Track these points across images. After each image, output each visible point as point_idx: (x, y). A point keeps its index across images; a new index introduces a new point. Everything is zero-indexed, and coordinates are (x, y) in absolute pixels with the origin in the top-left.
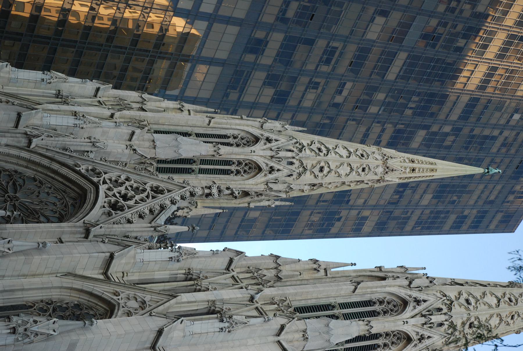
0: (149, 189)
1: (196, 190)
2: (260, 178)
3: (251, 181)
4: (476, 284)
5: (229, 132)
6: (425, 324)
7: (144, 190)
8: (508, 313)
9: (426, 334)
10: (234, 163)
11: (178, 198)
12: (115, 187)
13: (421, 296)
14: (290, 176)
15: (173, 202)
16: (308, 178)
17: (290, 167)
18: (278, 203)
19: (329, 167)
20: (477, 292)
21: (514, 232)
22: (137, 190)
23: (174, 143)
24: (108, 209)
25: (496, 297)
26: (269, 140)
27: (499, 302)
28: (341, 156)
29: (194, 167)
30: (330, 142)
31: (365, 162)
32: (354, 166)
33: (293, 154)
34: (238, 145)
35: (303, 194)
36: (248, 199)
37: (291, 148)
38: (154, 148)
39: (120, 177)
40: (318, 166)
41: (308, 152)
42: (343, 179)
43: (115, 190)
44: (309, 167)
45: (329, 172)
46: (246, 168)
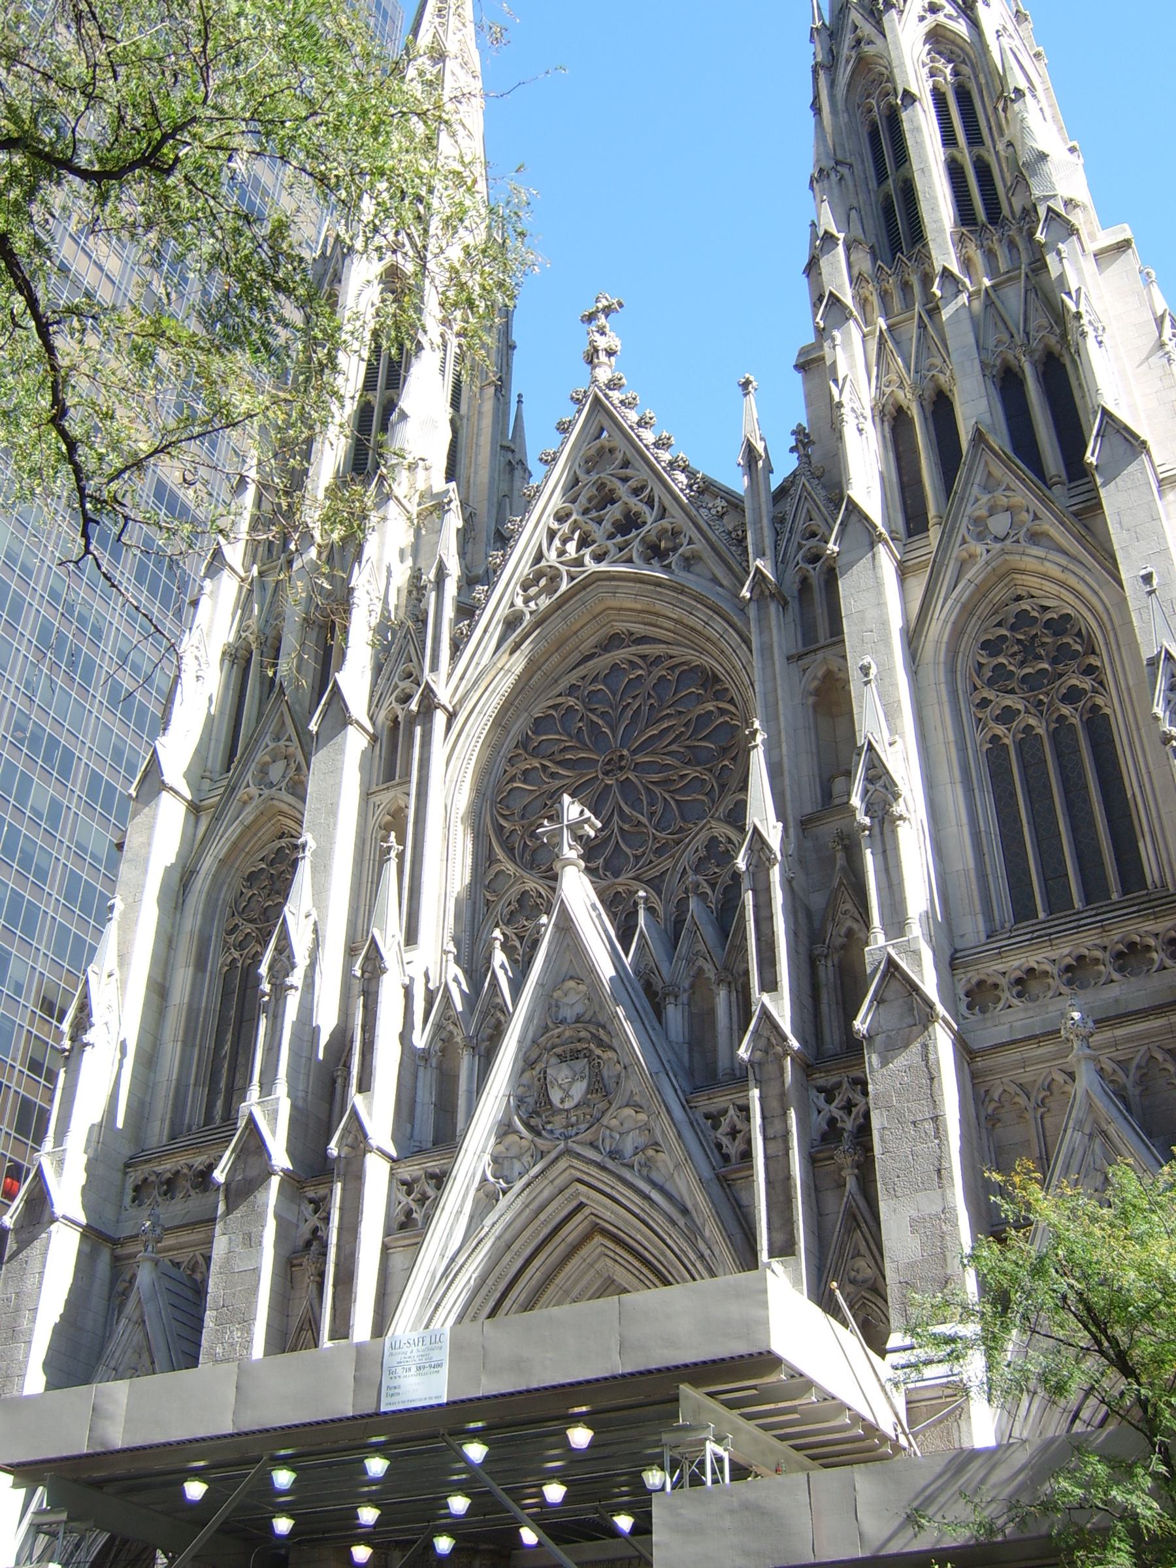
0: (594, 477)
24: (673, 559)
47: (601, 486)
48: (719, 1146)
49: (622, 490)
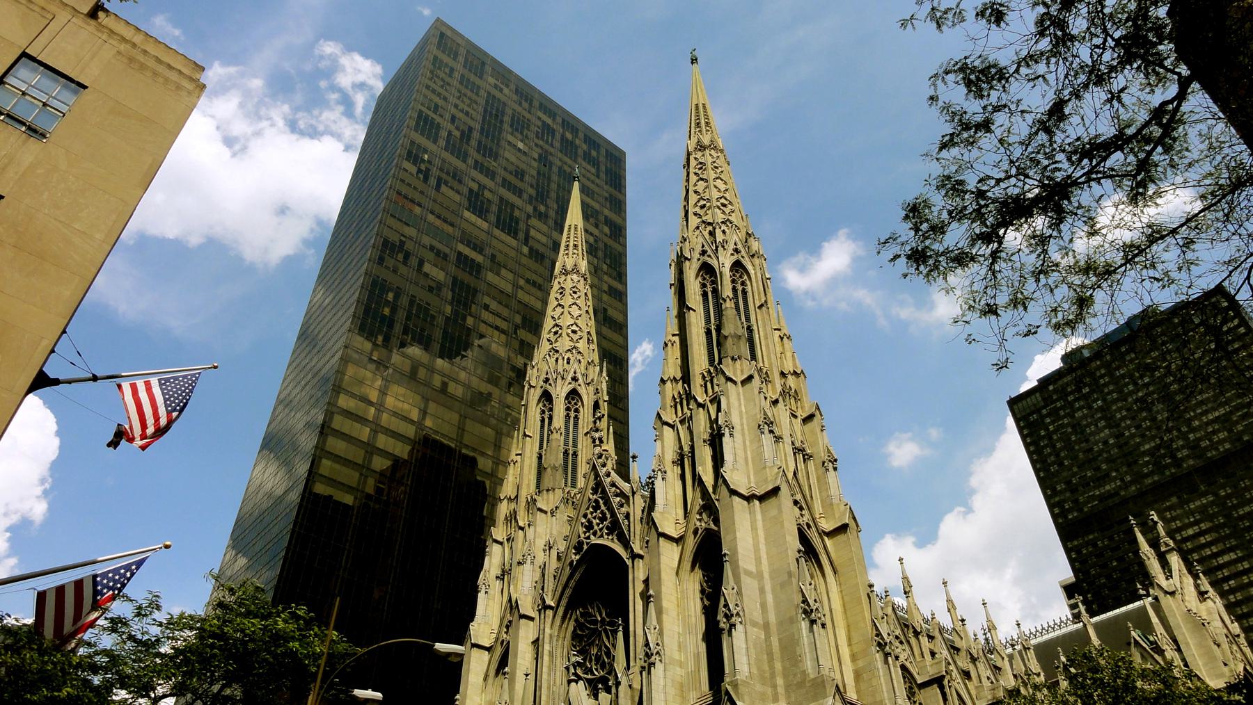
0: (595, 496)
1: (597, 452)
2: (582, 390)
3: (585, 398)
4: (687, 199)
5: (538, 417)
6: (723, 247)
7: (596, 501)
8: (712, 172)
9: (732, 246)
10: (568, 414)
11: (605, 469)
12: (592, 528)
13: (699, 249)
14: (580, 362)
15: (608, 475)
16: (582, 345)
17: (571, 362)
18: (604, 374)
19: (572, 325)
20: (693, 198)
21: (624, 153)
22: (597, 507)
23: (549, 470)
25: (698, 181)
26: (546, 381)
27: (702, 179)
28: (562, 313)
29: (571, 452)
30: (548, 324)
31: (568, 291)
32: (571, 301)
33: (560, 358)
34: (551, 410)
35: (596, 349)
36: (601, 402)
37: (553, 360)
38: (554, 489)
39: (582, 524)
40: (572, 335)
41: (557, 344)
42: (583, 312)
43: (596, 528)
44: (572, 344)
45: (577, 326)
46: (573, 402)
47: (596, 501)
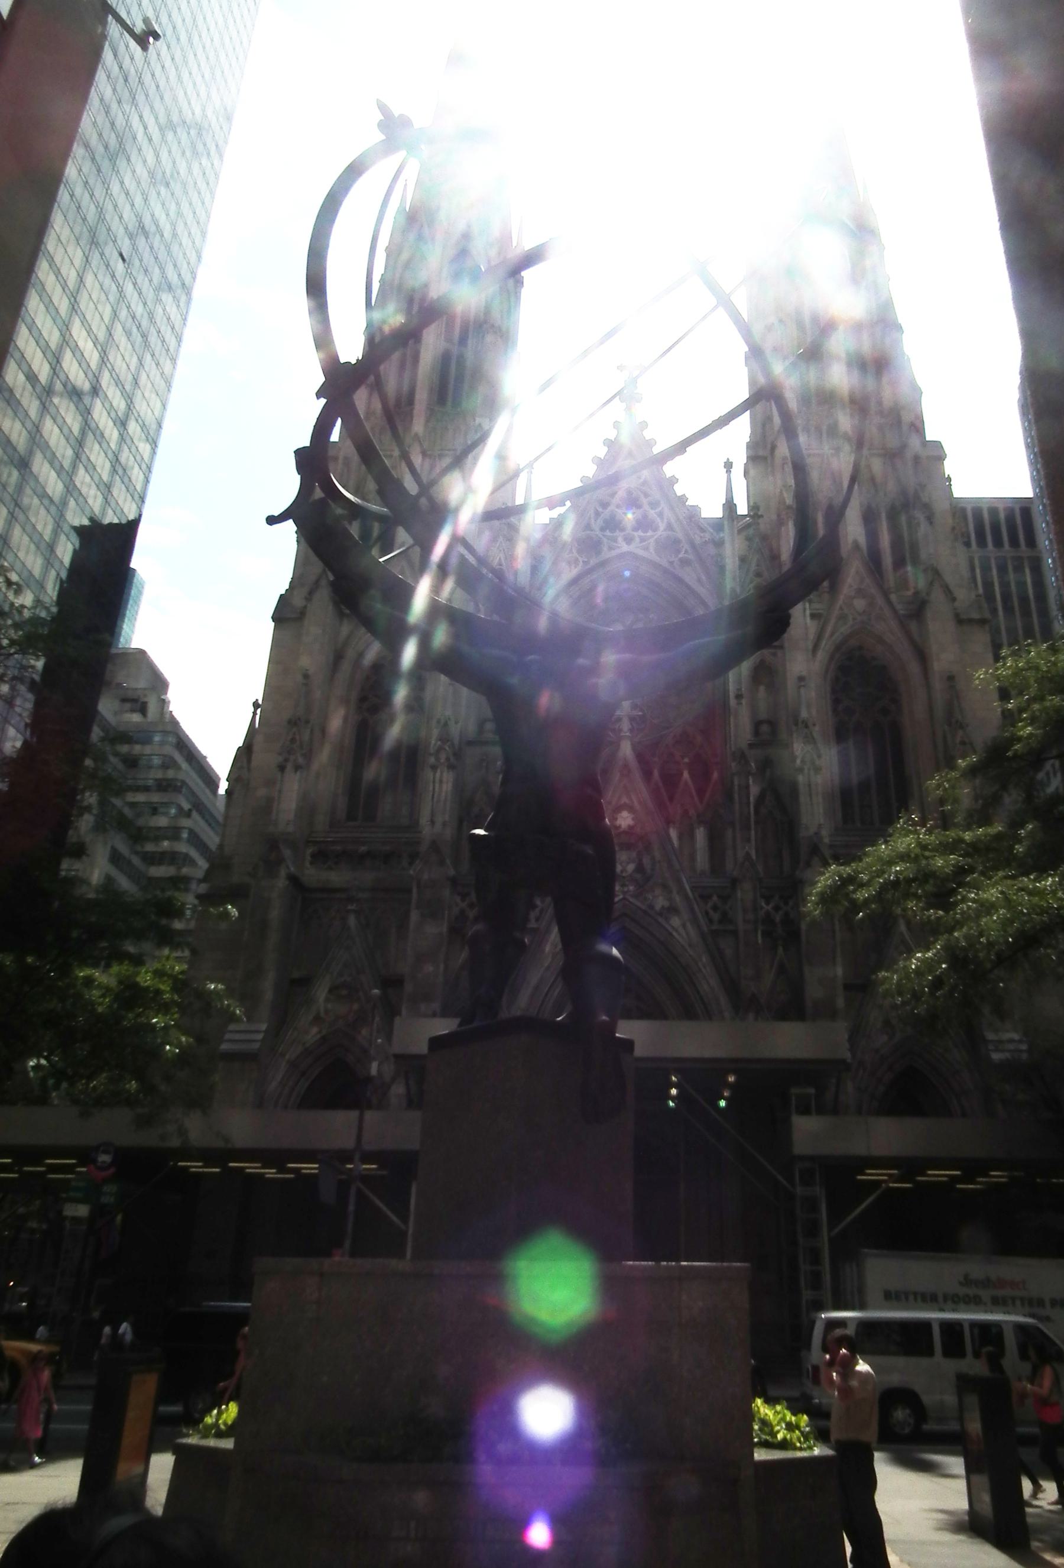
48: (707, 913)
49: (644, 501)
